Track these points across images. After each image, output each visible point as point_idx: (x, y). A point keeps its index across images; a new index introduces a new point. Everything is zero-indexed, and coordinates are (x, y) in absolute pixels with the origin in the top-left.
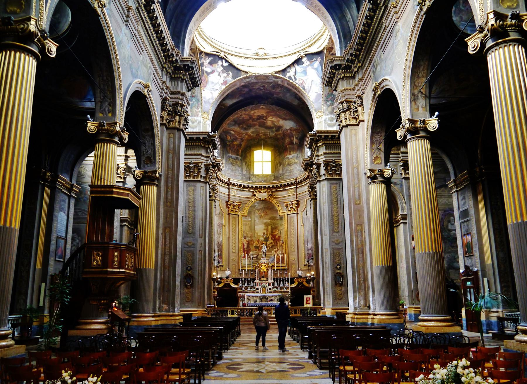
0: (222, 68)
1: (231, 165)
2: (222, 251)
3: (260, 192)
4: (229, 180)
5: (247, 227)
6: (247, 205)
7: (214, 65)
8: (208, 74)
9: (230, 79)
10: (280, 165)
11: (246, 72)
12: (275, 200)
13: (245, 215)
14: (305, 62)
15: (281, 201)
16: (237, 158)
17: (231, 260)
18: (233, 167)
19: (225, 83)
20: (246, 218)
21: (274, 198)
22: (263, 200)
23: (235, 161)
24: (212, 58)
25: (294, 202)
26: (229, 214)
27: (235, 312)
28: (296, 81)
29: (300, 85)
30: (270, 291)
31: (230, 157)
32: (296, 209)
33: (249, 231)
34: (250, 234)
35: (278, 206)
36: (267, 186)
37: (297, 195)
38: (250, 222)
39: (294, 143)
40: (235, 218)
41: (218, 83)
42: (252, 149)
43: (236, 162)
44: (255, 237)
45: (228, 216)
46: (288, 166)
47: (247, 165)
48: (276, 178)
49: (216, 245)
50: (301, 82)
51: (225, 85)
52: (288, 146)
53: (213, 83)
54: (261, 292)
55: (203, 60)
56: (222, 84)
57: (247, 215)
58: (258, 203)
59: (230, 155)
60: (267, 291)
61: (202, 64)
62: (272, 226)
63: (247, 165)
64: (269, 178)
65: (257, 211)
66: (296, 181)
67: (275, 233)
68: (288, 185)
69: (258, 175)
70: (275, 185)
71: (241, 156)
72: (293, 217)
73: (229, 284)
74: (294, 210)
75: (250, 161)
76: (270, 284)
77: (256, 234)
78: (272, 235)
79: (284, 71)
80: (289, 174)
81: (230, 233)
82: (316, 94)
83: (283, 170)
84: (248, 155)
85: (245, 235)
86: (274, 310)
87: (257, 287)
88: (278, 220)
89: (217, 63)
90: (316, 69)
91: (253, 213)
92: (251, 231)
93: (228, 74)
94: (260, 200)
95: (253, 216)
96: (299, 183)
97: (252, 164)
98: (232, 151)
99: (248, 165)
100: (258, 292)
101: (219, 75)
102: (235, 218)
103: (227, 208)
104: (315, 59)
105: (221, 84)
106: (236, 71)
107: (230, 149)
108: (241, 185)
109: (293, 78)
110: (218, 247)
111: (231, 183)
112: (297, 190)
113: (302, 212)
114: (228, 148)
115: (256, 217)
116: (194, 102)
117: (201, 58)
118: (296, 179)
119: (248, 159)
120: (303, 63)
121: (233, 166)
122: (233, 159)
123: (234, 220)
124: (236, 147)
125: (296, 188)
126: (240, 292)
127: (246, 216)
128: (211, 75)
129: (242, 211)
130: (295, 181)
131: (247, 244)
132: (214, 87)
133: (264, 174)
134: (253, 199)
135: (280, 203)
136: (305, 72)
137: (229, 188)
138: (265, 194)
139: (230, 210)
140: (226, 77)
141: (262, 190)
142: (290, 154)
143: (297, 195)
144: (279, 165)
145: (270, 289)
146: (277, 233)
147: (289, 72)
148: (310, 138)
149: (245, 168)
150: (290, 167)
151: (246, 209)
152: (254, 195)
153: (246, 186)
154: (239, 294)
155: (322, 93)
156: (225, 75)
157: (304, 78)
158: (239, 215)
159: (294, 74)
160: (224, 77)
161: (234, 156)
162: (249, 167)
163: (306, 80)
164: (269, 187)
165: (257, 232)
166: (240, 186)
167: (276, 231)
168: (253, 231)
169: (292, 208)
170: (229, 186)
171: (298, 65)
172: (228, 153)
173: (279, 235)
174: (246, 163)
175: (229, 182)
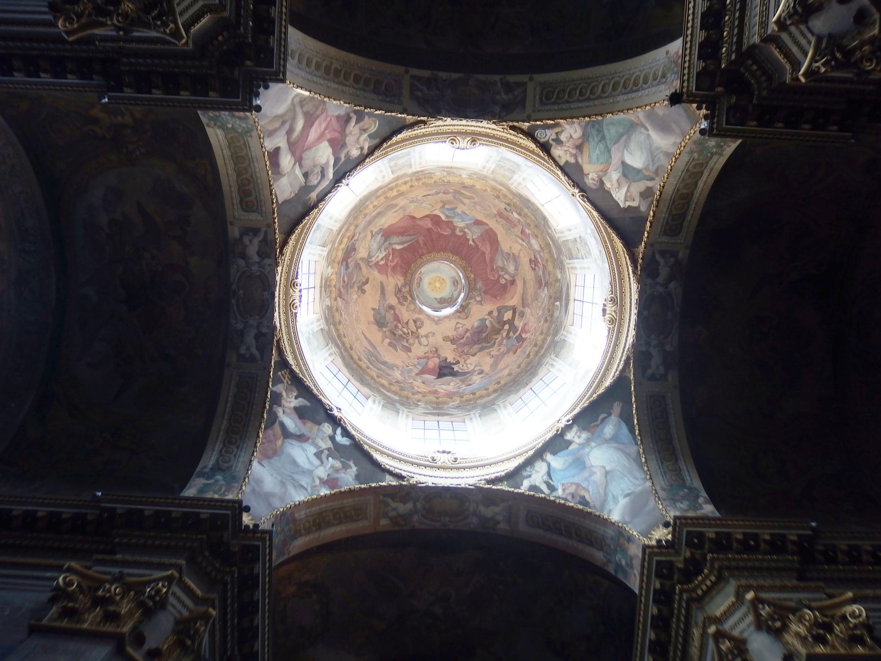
0: (329, 444)
7: (309, 424)
8: (286, 434)
9: (351, 479)
11: (400, 477)
14: (577, 440)
19: (330, 482)
24: (308, 404)
28: (554, 494)
29: (569, 498)
41: (310, 472)
50: (572, 489)
51: (332, 488)
53: (294, 463)
55: (279, 388)
56: (324, 483)
61: (277, 399)
79: (514, 476)
82: (627, 500)
89: (319, 424)
90: (614, 439)
93: (345, 467)
101: (318, 455)
104: (602, 416)
105: (317, 482)
106: (369, 466)
109: (544, 488)
116: (217, 481)
117: (277, 381)
120: (570, 443)
128: (295, 443)
132: (295, 476)
136: (579, 463)
140: (337, 471)
147: (530, 476)
148: (655, 559)
155: (649, 484)
156: (338, 464)
157: (576, 480)
159: (545, 478)
160: (332, 467)
163: (587, 479)
171: (554, 453)
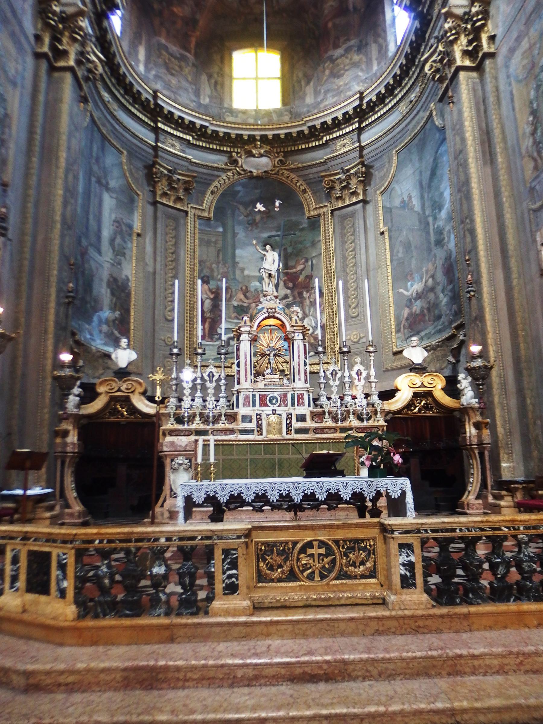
1: (165, 71)
2: (128, 311)
3: (250, 154)
4: (155, 97)
5: (212, 251)
6: (211, 188)
10: (308, 83)
12: (292, 176)
13: (206, 214)
15: (311, 176)
16: (183, 58)
17: (156, 341)
18: (169, 77)
20: (209, 225)
21: (292, 170)
22: (258, 177)
23: (177, 62)
25: (352, 171)
26: (155, 203)
27: (55, 572)
30: (300, 425)
31: (161, 47)
32: (360, 191)
33: (218, 263)
34: (221, 271)
35: (304, 191)
36: (270, 134)
37: (362, 148)
38: (220, 238)
39: (351, 7)
40: (176, 220)
42: (227, 44)
43: (180, 67)
44: (235, 279)
45: (150, 209)
46: (332, 80)
47: (213, 81)
48: (295, 115)
49: (104, 285)
52: (330, 25)
54: (260, 432)
57: (212, 215)
58: (244, 185)
59: (163, 41)
60: (289, 426)
62: (285, 249)
63: (213, 81)
64: (275, 118)
65: (241, 207)
66: (360, 105)
67: (294, 267)
68: (337, 124)
69: (244, 112)
70: (294, 131)
71: (196, 55)
72: (353, 215)
73: (126, 401)
74: (354, 193)
75: (221, 74)
76: (300, 397)
77: (238, 272)
78: (286, 274)
80: (334, 100)
81: (158, 259)
83: (316, 93)
84: (217, 57)
85: (206, 272)
86: (404, 546)
87: (243, 411)
88: (303, 229)
91: (229, 212)
92: (225, 264)
94: (251, 177)
95: (229, 222)
96: (372, 107)
97: (227, 83)
98: (168, 33)
99: (216, 83)
100: (251, 431)
102: (176, 220)
103: (149, 185)
107: (162, 24)
108: (193, 123)
110: (113, 294)
111: (162, 108)
112: (362, 137)
113: (382, 193)
114: (157, 22)
115: (240, 223)
118: (361, 98)
119: (216, 69)
121: (172, 74)
122: (171, 55)
123: (172, 223)
124: (179, 24)
125: (360, 130)
126: (172, 433)
127: (209, 219)
129: (198, 204)
130: (357, 103)
131: (212, 299)
133: (260, 108)
134: (230, 174)
135: (308, 184)
137: (156, 130)
138: (264, 160)
139: (159, 192)
141: (255, 147)
142: (336, 46)
143: (362, 148)
144: (303, 83)
145: (302, 418)
146: (302, 266)
149: (206, 90)
150: (336, 80)
151: (209, 200)
152: (235, 162)
153: (209, 132)
154: (169, 439)
158: (186, 213)
161: (174, 49)
162: (219, 87)
164: (276, 137)
165: (241, 265)
166: (190, 128)
167: (297, 262)
168: (230, 261)
169: (347, 187)
170: (156, 122)
172: (157, 33)
173: (308, 271)
174: (210, 76)
175: (157, 105)
